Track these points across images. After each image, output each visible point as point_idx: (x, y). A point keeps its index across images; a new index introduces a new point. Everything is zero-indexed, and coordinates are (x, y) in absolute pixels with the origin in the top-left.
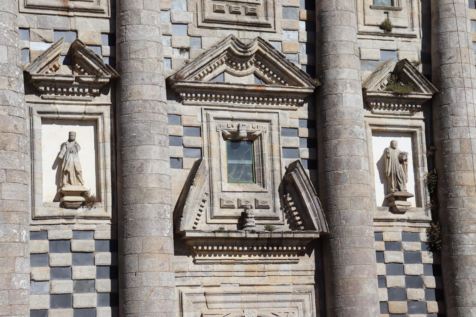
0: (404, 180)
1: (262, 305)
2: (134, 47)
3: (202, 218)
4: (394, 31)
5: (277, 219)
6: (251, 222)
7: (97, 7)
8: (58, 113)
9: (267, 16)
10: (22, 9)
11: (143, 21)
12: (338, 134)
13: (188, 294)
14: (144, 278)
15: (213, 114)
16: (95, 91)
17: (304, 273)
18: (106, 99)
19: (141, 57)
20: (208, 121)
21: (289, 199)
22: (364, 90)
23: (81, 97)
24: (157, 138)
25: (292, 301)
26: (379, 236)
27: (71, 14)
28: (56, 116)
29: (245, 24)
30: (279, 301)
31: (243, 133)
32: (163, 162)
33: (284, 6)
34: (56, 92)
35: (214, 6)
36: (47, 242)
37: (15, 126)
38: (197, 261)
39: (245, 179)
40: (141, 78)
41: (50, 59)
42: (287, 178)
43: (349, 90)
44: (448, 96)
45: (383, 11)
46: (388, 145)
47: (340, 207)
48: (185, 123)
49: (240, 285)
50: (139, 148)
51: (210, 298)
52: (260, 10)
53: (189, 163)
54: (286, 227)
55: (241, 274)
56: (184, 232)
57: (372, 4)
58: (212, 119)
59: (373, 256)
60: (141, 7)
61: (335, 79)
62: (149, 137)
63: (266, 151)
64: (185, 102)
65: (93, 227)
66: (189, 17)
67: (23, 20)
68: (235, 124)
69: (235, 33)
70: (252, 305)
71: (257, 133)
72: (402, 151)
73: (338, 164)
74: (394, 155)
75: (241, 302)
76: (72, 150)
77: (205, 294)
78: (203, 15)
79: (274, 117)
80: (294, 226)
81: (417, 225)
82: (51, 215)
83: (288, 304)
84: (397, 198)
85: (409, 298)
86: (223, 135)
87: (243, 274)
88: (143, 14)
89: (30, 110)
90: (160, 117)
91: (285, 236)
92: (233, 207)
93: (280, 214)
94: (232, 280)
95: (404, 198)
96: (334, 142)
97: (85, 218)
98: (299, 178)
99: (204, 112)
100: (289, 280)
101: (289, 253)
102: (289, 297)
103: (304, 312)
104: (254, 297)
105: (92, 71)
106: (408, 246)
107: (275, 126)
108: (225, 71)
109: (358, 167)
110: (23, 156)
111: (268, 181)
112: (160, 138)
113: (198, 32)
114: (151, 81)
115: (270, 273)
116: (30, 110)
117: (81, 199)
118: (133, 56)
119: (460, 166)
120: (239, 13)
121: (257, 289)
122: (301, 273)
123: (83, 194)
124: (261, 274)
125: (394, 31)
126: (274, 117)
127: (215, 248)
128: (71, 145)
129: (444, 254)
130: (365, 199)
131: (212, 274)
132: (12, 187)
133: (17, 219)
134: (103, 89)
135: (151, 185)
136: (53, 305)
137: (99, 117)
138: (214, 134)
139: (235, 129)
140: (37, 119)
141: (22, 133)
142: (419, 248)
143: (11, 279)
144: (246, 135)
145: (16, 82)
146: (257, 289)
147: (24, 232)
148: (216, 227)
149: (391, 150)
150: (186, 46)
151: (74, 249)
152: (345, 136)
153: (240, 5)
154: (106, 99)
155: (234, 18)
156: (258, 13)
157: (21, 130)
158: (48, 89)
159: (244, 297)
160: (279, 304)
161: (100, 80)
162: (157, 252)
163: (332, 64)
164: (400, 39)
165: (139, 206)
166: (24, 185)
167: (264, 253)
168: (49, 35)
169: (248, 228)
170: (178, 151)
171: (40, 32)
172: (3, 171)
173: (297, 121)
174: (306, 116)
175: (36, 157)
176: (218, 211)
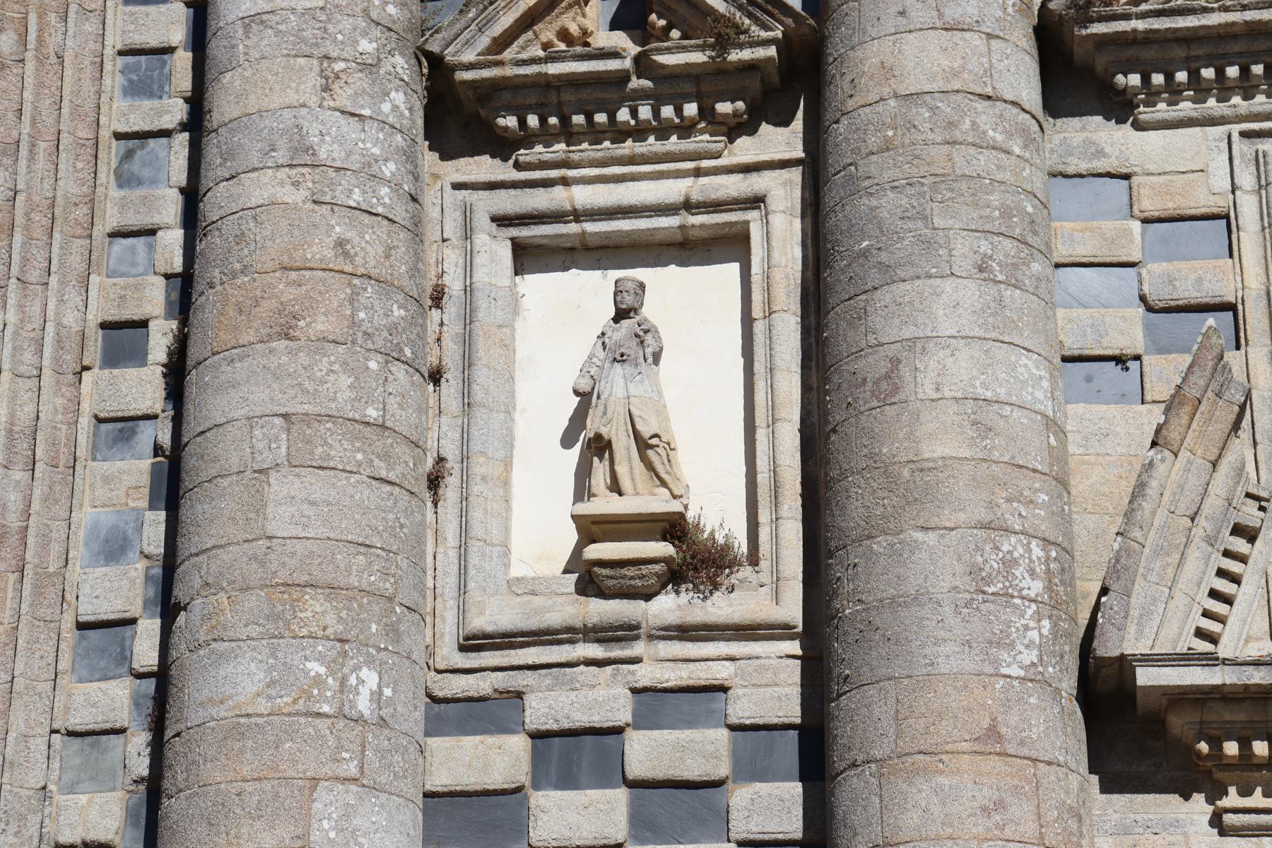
16: (724, 108)
24: (964, 249)
32: (1000, 351)
34: (569, 134)
36: (518, 744)
37: (340, 243)
38: (1229, 819)
40: (893, 10)
48: (1150, 204)
50: (884, 297)
56: (1124, 665)
64: (1145, 113)
65: (720, 672)
76: (623, 350)
82: (533, 624)
89: (467, 213)
97: (685, 632)
99: (1239, 145)
110: (373, 365)
112: (985, 247)
114: (941, 16)
116: (467, 213)
117: (663, 549)
132: (316, 486)
133: (330, 619)
135: (934, 449)
137: (752, 215)
141: (374, 272)
145: (359, 80)
147: (371, 678)
158: (533, 121)
161: (735, 56)
162: (965, 746)
165: (879, 545)
166: (374, 482)
172: (278, 421)
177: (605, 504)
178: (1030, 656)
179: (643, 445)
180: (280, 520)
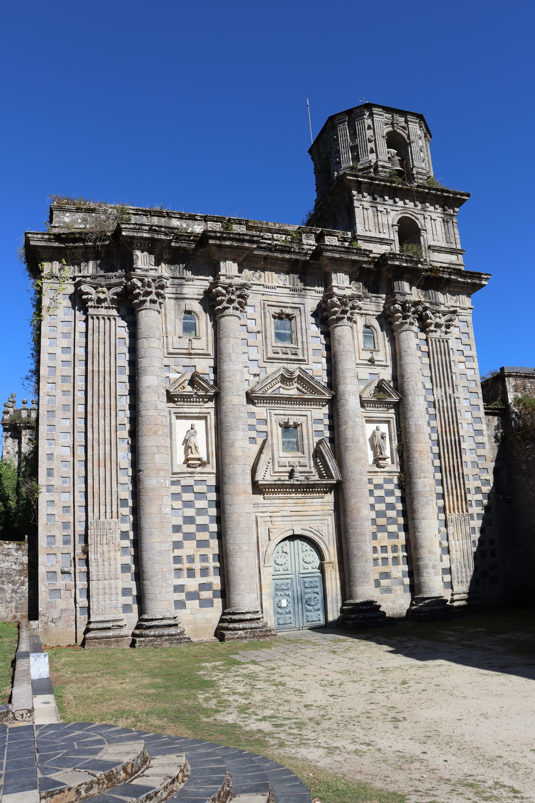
0: (384, 449)
1: (304, 522)
2: (227, 374)
3: (268, 473)
4: (376, 363)
5: (312, 472)
6: (297, 475)
7: (207, 352)
8: (185, 413)
9: (303, 355)
12: (346, 422)
15: (273, 412)
16: (205, 400)
17: (327, 504)
18: (212, 404)
19: (231, 380)
20: (271, 416)
21: (318, 461)
22: (360, 397)
23: (198, 404)
24: (241, 427)
26: (370, 481)
27: (192, 357)
28: (184, 415)
29: (291, 360)
30: (313, 520)
31: (291, 423)
34: (184, 401)
35: (273, 350)
36: (180, 487)
39: (293, 449)
41: (181, 382)
42: (317, 449)
43: (352, 397)
44: (408, 399)
45: (369, 352)
46: (375, 429)
47: (348, 465)
48: (257, 418)
49: (291, 511)
50: (231, 432)
51: (273, 519)
52: (300, 352)
53: (260, 441)
54: (317, 477)
55: (291, 505)
56: (258, 481)
57: (363, 348)
58: (273, 415)
59: (367, 493)
60: (232, 352)
62: (237, 426)
63: (305, 433)
65: (205, 479)
66: (259, 357)
67: (166, 362)
68: (286, 417)
69: (285, 365)
70: (298, 522)
71: (299, 423)
72: (383, 432)
73: (346, 440)
74: (378, 434)
77: (270, 517)
78: (267, 355)
79: (308, 413)
80: (321, 476)
81: (392, 474)
82: (182, 471)
83: (318, 522)
84: (380, 459)
85: (388, 516)
86: (279, 424)
87: (292, 505)
88: (233, 355)
89: (170, 412)
90: (243, 414)
91: (316, 482)
92: (285, 466)
93: (313, 470)
94: (286, 508)
95: (384, 459)
96: (344, 427)
97: (201, 473)
98: (324, 448)
100: (319, 508)
101: (319, 492)
103: (328, 526)
104: (299, 518)
105: (204, 389)
106: (387, 486)
107: (309, 419)
108: (280, 387)
109: (358, 441)
111: (306, 451)
113: (264, 365)
115: (308, 504)
116: (170, 412)
117: (199, 462)
118: (227, 380)
119: (415, 440)
120: (287, 354)
121: (300, 513)
122: (326, 504)
123: (199, 459)
124: (303, 505)
125: (376, 363)
126: (308, 413)
127: (276, 490)
128: (192, 431)
129: (407, 491)
130: (362, 460)
131: (274, 505)
134: (210, 399)
135: (238, 454)
136: (184, 523)
137: (208, 415)
138: (274, 424)
140: (174, 417)
142: (393, 488)
143: (161, 508)
146: (300, 513)
148: (276, 478)
149: (377, 431)
150: (257, 373)
151: (195, 491)
152: (350, 423)
153: (288, 349)
154: (212, 404)
155: (284, 356)
157: (164, 423)
158: (179, 399)
159: (293, 518)
160: (313, 522)
161: (208, 394)
163: (342, 382)
165: (231, 466)
167: (304, 492)
168: (180, 369)
170: (254, 434)
171: (175, 368)
173: (323, 415)
174: (328, 413)
175: (173, 438)
176: (277, 469)
179: (196, 448)
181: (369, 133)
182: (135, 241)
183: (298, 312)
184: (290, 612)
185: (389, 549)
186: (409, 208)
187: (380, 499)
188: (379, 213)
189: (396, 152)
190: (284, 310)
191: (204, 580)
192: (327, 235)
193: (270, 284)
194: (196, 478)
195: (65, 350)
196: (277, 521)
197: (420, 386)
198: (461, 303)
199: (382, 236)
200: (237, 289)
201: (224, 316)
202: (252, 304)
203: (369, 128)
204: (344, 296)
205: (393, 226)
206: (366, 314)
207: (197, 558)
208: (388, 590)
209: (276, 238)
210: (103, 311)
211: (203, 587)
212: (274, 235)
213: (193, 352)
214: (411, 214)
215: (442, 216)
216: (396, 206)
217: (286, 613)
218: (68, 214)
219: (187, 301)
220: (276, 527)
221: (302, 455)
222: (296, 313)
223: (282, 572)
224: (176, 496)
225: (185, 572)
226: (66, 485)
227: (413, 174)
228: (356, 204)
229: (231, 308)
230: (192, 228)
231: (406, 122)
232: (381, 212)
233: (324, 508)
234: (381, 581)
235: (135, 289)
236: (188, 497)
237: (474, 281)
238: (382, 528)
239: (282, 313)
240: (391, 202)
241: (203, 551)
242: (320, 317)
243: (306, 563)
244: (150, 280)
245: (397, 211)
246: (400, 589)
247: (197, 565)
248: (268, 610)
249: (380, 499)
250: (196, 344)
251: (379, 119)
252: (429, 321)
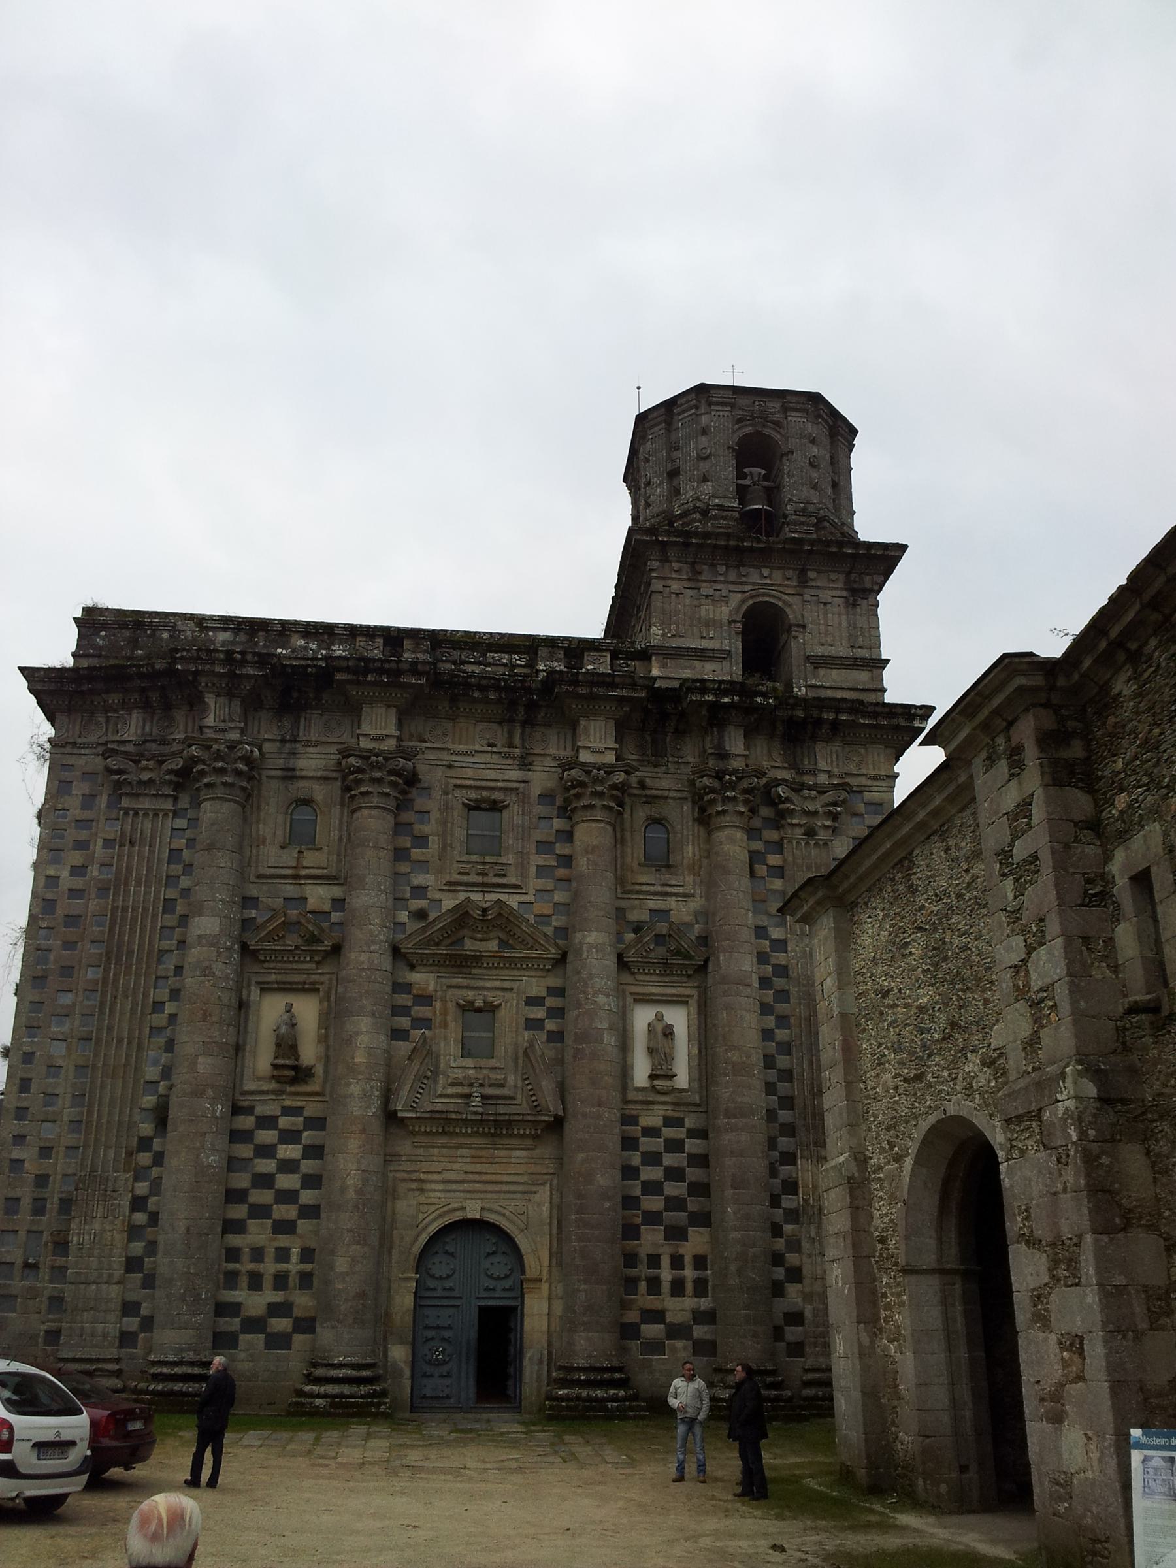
1: (489, 1196)
10: (253, 879)
11: (367, 887)
13: (404, 1180)
14: (342, 1161)
22: (620, 957)
25: (525, 1192)
26: (629, 1120)
30: (509, 1192)
33: (537, 866)
36: (252, 1118)
37: (219, 997)
49: (466, 1173)
51: (428, 1186)
52: (511, 870)
55: (465, 1160)
56: (396, 1112)
61: (580, 942)
67: (253, 891)
75: (463, 1191)
77: (422, 1181)
79: (515, 985)
82: (259, 1089)
83: (519, 1196)
87: (468, 1160)
92: (460, 1084)
94: (456, 1166)
100: (522, 1169)
102: (521, 1188)
106: (669, 1132)
113: (438, 895)
116: (249, 980)
117: (293, 1073)
121: (484, 1178)
123: (294, 1068)
139: (469, 998)
143: (198, 1156)
144: (482, 1004)
146: (484, 1178)
147: (220, 1107)
155: (479, 879)
156: (508, 874)
159: (466, 1186)
160: (508, 1196)
164: (674, 898)
169: (472, 1109)
177: (281, 1062)
178: (374, 1110)
180: (201, 1068)
181: (704, 440)
182: (203, 681)
183: (514, 797)
184: (448, 1375)
185: (665, 1261)
186: (772, 585)
187: (652, 1159)
188: (703, 601)
189: (763, 472)
190: (485, 794)
191: (277, 1297)
192: (589, 650)
193: (462, 747)
194: (287, 1103)
195: (78, 871)
196: (435, 1191)
197: (747, 934)
198: (871, 767)
199: (704, 644)
200: (385, 758)
201: (360, 808)
202: (426, 785)
203: (704, 432)
204: (594, 766)
205: (730, 622)
206: (656, 797)
207: (270, 1252)
208: (656, 1347)
209: (491, 661)
210: (146, 803)
211: (275, 1310)
212: (490, 655)
213: (303, 872)
214: (773, 596)
215: (845, 594)
216: (742, 583)
217: (442, 1376)
218: (103, 633)
219: (302, 784)
220: (434, 1201)
221: (498, 1065)
222: (510, 799)
223: (440, 1293)
224: (237, 1136)
225: (244, 1281)
226: (50, 1109)
227: (785, 516)
228: (657, 585)
229: (376, 794)
230: (328, 649)
231: (785, 409)
232: (707, 596)
233: (534, 1169)
234: (643, 1327)
235: (196, 763)
236: (266, 1136)
237: (894, 721)
238: (653, 1218)
239: (483, 800)
240: (732, 576)
241: (283, 1241)
242: (557, 804)
243: (491, 1277)
244: (222, 747)
245: (744, 592)
246: (685, 1348)
247: (269, 1267)
248: (402, 1365)
249: (652, 1159)
250: (311, 858)
251: (721, 414)
252: (781, 806)
